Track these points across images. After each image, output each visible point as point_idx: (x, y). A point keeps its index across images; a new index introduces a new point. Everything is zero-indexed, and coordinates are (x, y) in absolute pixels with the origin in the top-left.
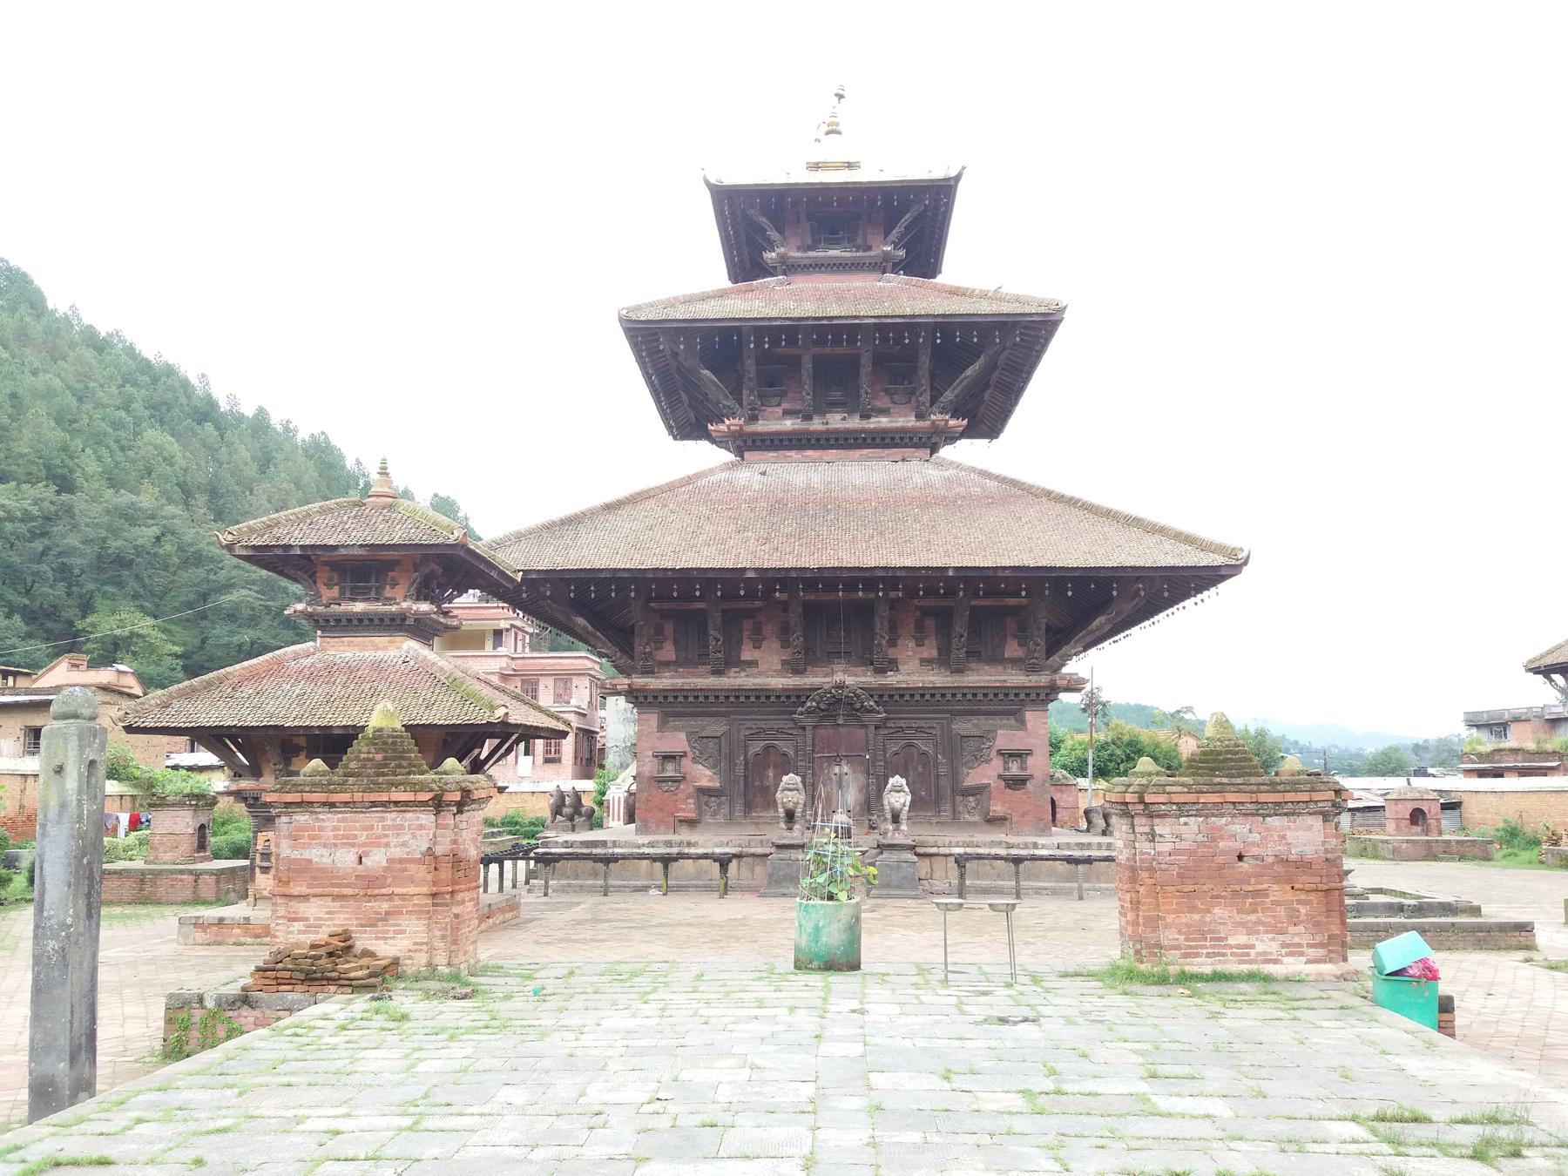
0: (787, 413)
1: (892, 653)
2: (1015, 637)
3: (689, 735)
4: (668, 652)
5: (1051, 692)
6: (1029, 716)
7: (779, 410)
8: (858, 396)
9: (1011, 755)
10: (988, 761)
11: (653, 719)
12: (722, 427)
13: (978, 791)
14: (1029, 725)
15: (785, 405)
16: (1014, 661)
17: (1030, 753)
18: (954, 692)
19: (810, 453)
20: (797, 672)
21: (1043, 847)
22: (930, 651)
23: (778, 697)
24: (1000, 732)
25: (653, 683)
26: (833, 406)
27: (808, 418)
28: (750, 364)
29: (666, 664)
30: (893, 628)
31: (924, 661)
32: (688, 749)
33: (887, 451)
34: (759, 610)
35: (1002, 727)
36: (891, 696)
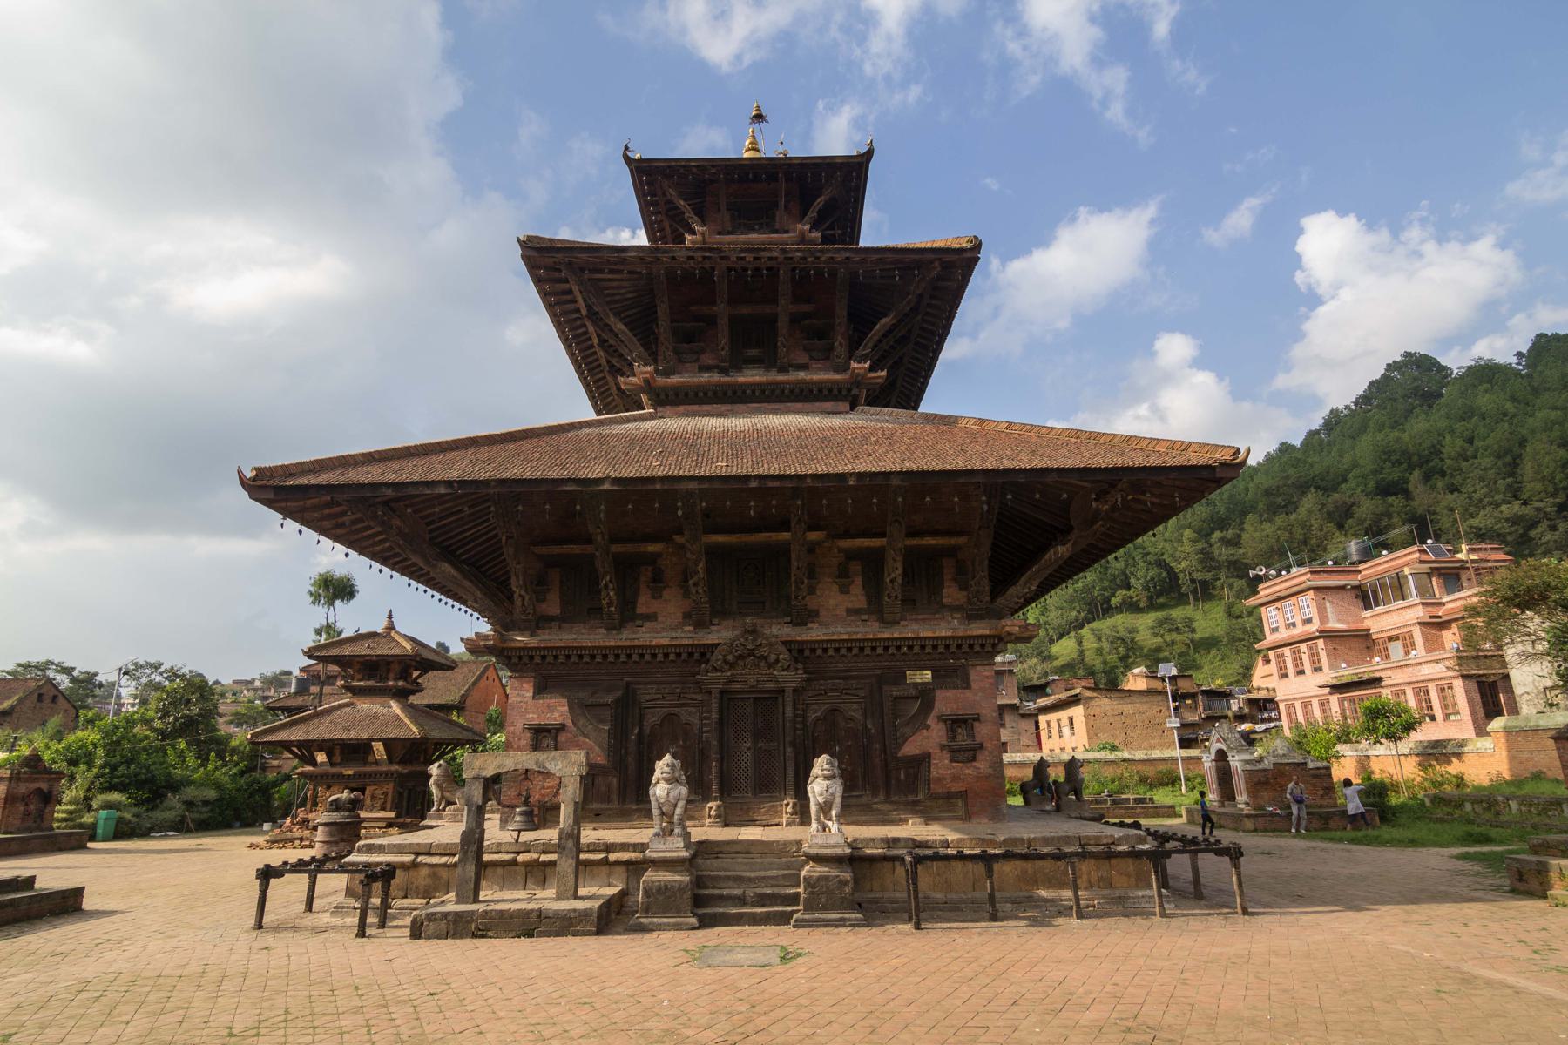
1: (811, 602)
2: (955, 580)
4: (552, 607)
5: (997, 643)
8: (776, 347)
9: (954, 721)
12: (634, 379)
16: (953, 609)
17: (977, 719)
18: (887, 644)
20: (700, 624)
22: (857, 597)
27: (724, 371)
28: (662, 310)
29: (550, 619)
30: (812, 573)
31: (850, 612)
32: (569, 723)
34: (658, 555)
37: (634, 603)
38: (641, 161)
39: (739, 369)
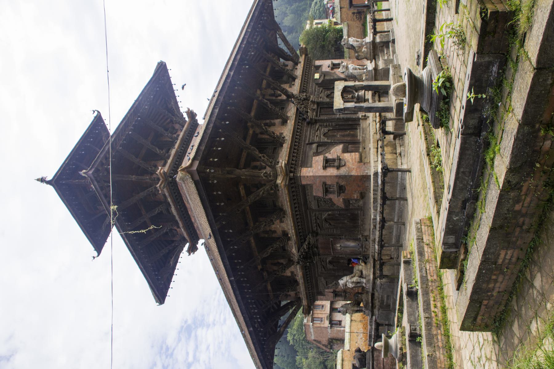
0: (179, 227)
3: (325, 288)
6: (304, 182)
7: (178, 230)
10: (331, 199)
11: (319, 297)
13: (347, 202)
14: (309, 183)
15: (175, 228)
19: (193, 220)
21: (375, 216)
23: (306, 270)
24: (314, 194)
25: (305, 302)
26: (170, 213)
33: (183, 195)
35: (312, 193)
36: (300, 236)
37: (287, 277)
38: (96, 250)
39: (174, 217)
